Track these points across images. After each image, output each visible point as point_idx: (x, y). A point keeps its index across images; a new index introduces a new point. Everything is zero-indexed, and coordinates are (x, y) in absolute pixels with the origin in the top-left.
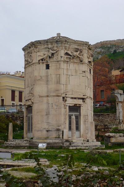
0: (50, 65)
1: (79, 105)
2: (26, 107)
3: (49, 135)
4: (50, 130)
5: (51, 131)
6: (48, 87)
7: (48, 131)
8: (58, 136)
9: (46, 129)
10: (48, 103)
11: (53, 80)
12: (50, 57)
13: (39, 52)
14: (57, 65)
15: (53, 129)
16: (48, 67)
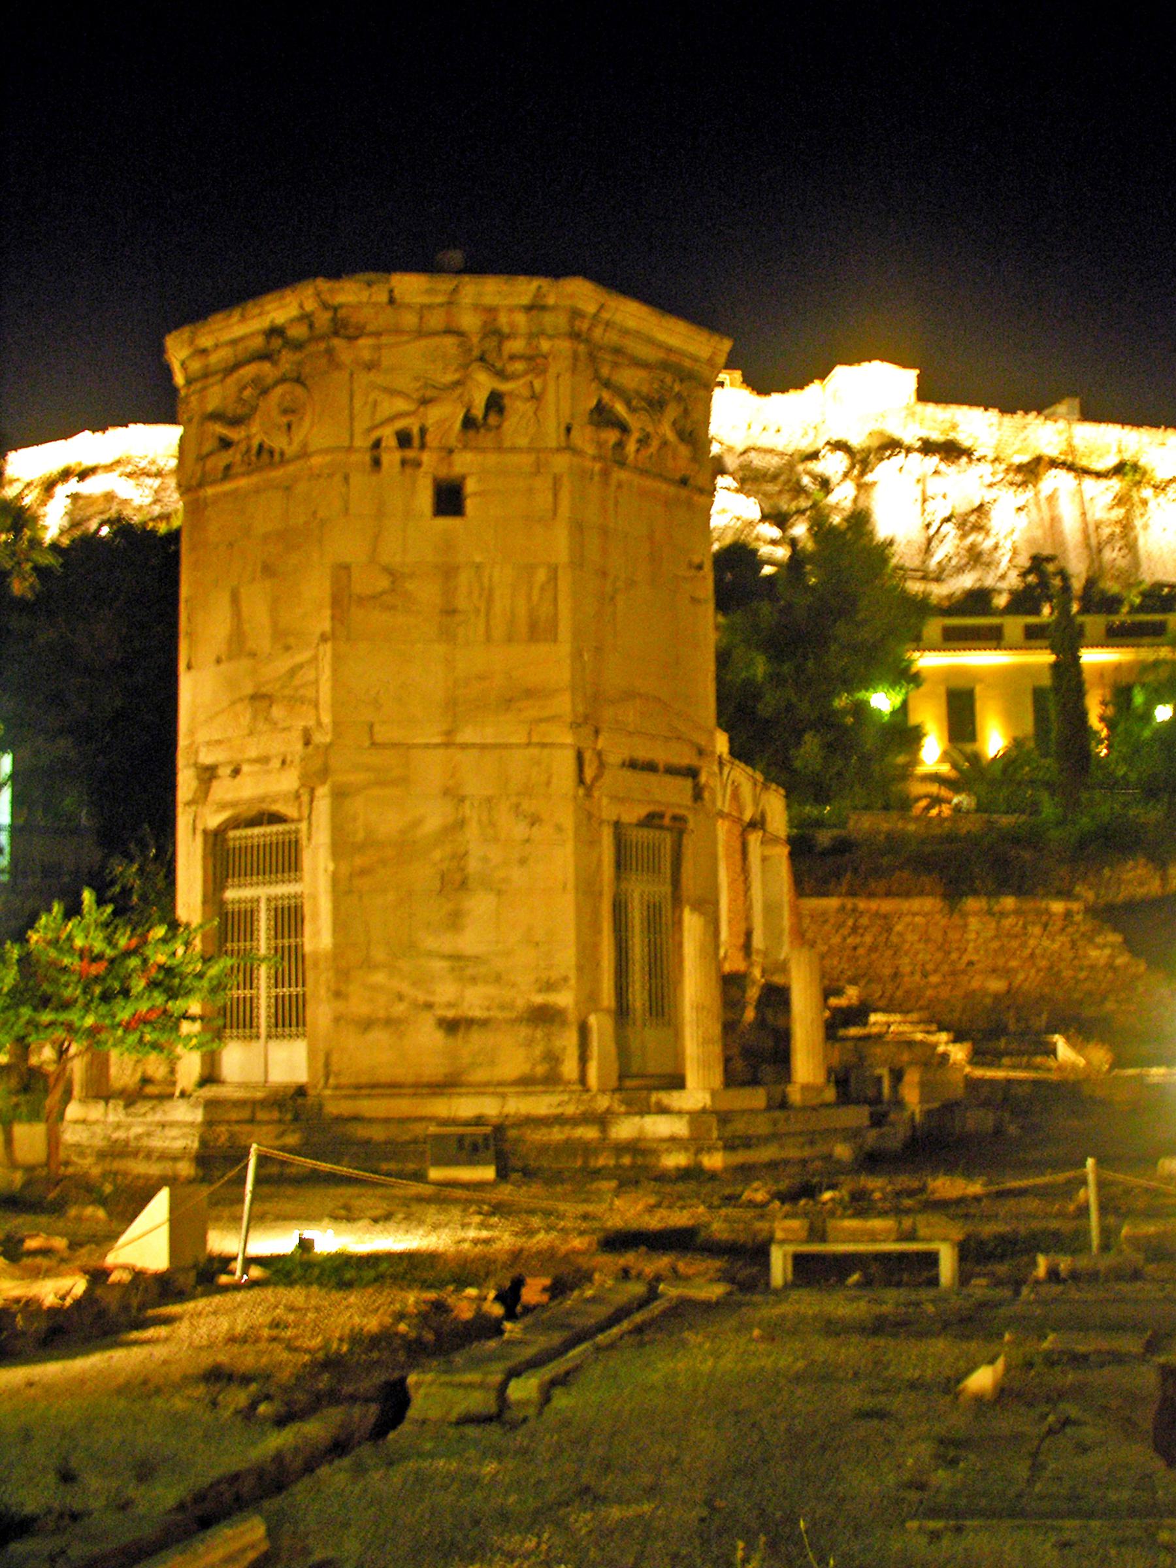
0: (471, 486)
1: (675, 818)
2: (214, 821)
3: (467, 1060)
4: (470, 1022)
5: (484, 1023)
6: (449, 663)
7: (452, 1026)
8: (540, 1070)
9: (441, 1012)
10: (453, 794)
11: (498, 607)
12: (469, 423)
13: (371, 366)
14: (530, 490)
15: (502, 1007)
16: (449, 499)
